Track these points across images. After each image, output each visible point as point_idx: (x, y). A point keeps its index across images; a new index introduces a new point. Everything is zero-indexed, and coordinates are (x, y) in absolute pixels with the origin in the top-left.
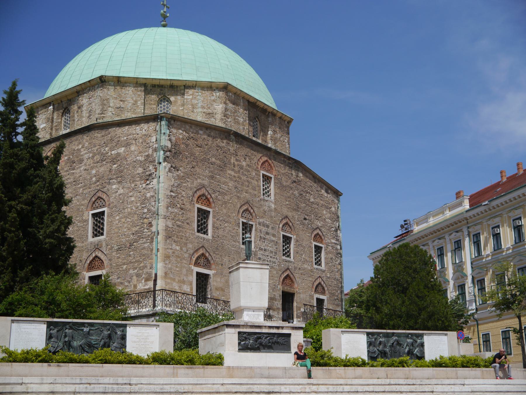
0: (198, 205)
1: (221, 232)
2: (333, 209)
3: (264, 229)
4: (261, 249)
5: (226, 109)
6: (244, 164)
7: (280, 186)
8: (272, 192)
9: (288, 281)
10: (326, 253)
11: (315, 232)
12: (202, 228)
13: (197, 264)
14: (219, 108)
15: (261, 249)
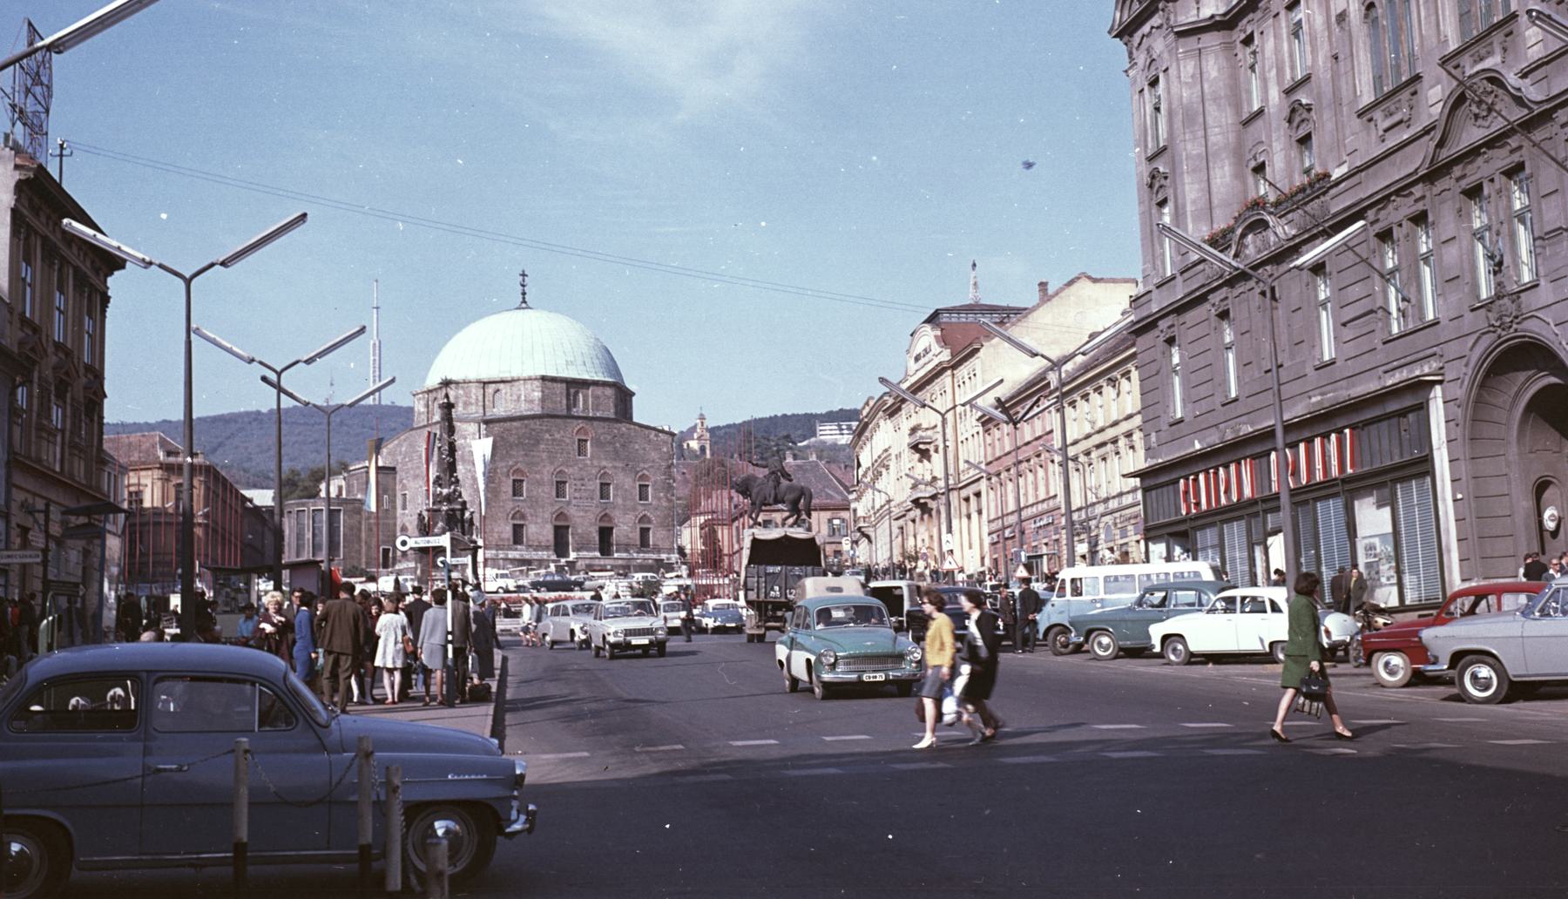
0: (512, 478)
1: (535, 493)
2: (665, 450)
3: (579, 483)
4: (575, 498)
5: (543, 396)
6: (557, 436)
7: (598, 443)
8: (589, 451)
9: (606, 519)
10: (655, 490)
11: (640, 474)
12: (517, 491)
13: (513, 518)
14: (537, 395)
15: (575, 498)
